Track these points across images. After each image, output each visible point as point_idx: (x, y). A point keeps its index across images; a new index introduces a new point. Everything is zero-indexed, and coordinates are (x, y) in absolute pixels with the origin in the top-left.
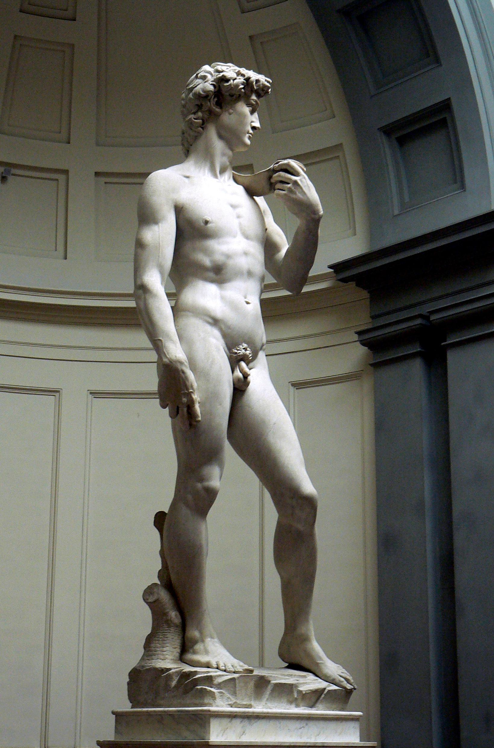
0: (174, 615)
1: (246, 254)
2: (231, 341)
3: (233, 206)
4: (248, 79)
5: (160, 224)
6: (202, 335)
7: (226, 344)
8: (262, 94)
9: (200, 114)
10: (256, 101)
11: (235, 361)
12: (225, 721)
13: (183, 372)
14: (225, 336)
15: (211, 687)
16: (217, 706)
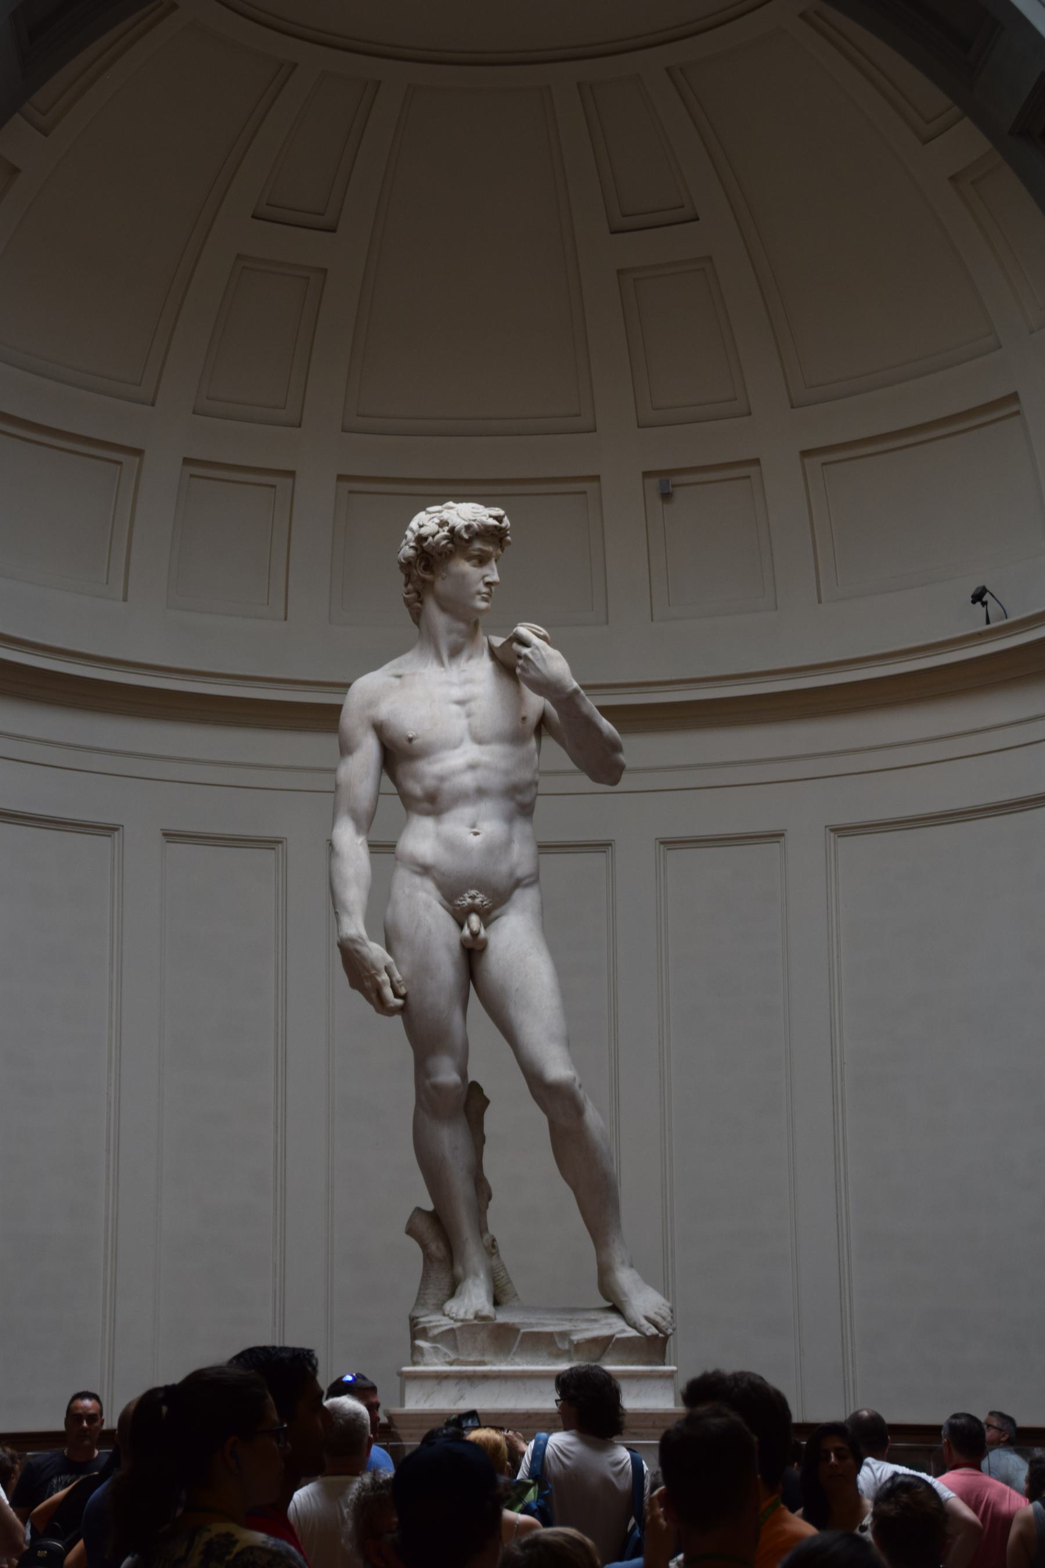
0: (436, 1248)
1: (472, 767)
2: (451, 891)
3: (461, 703)
4: (452, 530)
5: (354, 754)
6: (407, 891)
7: (444, 896)
8: (496, 533)
9: (410, 587)
10: (480, 550)
11: (460, 918)
12: (430, 1384)
13: (357, 952)
14: (440, 886)
15: (426, 1341)
16: (426, 1365)
